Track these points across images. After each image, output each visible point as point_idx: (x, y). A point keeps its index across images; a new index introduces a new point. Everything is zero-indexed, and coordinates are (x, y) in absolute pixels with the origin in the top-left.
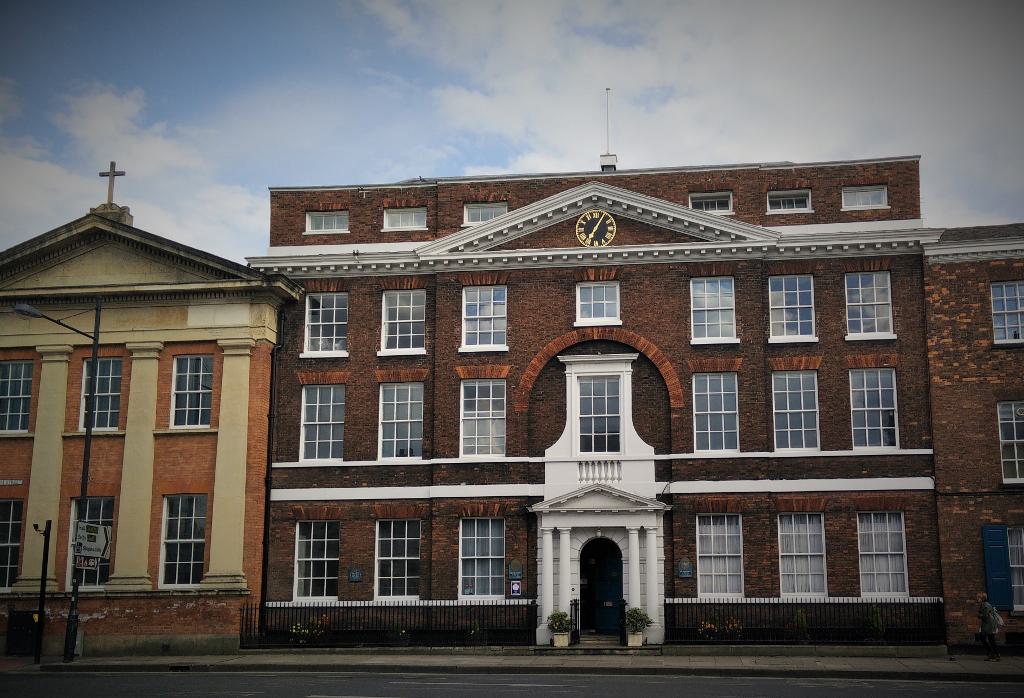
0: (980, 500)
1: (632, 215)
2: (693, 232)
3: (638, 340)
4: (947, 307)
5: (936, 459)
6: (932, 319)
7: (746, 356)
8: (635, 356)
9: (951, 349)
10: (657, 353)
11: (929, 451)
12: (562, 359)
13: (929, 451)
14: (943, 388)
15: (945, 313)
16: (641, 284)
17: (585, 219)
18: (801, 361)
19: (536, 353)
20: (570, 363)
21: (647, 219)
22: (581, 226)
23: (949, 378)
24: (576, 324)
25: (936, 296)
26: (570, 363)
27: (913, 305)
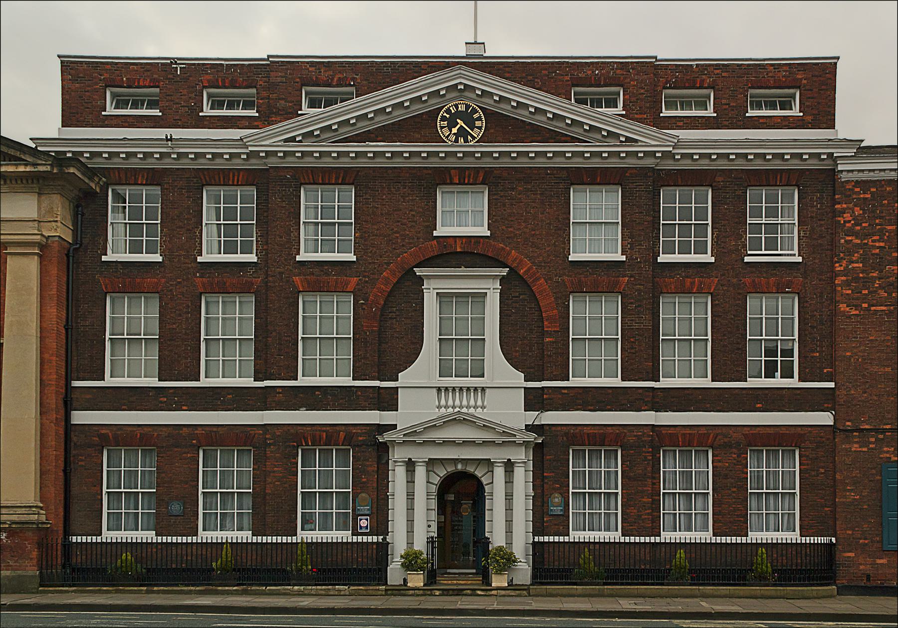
0: (881, 436)
1: (504, 109)
2: (576, 132)
3: (509, 254)
4: (858, 228)
5: (838, 393)
6: (842, 241)
7: (631, 277)
8: (504, 272)
9: (861, 275)
10: (529, 269)
11: (831, 385)
12: (418, 272)
13: (831, 385)
14: (849, 317)
15: (856, 235)
16: (513, 189)
17: (448, 111)
18: (692, 284)
19: (388, 264)
20: (429, 277)
21: (523, 115)
22: (443, 119)
23: (857, 307)
24: (435, 234)
25: (847, 216)
26: (429, 277)
27: (821, 225)
